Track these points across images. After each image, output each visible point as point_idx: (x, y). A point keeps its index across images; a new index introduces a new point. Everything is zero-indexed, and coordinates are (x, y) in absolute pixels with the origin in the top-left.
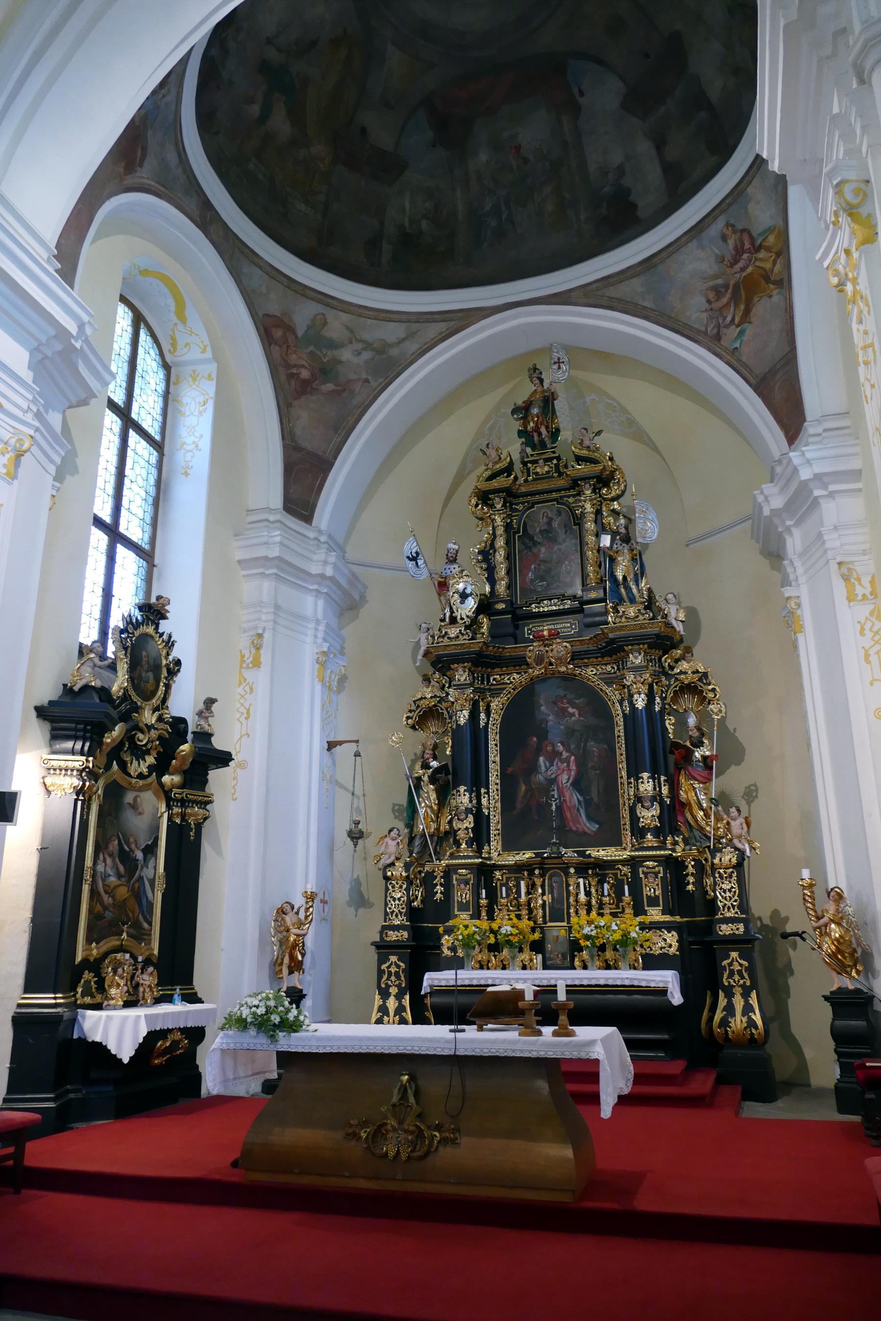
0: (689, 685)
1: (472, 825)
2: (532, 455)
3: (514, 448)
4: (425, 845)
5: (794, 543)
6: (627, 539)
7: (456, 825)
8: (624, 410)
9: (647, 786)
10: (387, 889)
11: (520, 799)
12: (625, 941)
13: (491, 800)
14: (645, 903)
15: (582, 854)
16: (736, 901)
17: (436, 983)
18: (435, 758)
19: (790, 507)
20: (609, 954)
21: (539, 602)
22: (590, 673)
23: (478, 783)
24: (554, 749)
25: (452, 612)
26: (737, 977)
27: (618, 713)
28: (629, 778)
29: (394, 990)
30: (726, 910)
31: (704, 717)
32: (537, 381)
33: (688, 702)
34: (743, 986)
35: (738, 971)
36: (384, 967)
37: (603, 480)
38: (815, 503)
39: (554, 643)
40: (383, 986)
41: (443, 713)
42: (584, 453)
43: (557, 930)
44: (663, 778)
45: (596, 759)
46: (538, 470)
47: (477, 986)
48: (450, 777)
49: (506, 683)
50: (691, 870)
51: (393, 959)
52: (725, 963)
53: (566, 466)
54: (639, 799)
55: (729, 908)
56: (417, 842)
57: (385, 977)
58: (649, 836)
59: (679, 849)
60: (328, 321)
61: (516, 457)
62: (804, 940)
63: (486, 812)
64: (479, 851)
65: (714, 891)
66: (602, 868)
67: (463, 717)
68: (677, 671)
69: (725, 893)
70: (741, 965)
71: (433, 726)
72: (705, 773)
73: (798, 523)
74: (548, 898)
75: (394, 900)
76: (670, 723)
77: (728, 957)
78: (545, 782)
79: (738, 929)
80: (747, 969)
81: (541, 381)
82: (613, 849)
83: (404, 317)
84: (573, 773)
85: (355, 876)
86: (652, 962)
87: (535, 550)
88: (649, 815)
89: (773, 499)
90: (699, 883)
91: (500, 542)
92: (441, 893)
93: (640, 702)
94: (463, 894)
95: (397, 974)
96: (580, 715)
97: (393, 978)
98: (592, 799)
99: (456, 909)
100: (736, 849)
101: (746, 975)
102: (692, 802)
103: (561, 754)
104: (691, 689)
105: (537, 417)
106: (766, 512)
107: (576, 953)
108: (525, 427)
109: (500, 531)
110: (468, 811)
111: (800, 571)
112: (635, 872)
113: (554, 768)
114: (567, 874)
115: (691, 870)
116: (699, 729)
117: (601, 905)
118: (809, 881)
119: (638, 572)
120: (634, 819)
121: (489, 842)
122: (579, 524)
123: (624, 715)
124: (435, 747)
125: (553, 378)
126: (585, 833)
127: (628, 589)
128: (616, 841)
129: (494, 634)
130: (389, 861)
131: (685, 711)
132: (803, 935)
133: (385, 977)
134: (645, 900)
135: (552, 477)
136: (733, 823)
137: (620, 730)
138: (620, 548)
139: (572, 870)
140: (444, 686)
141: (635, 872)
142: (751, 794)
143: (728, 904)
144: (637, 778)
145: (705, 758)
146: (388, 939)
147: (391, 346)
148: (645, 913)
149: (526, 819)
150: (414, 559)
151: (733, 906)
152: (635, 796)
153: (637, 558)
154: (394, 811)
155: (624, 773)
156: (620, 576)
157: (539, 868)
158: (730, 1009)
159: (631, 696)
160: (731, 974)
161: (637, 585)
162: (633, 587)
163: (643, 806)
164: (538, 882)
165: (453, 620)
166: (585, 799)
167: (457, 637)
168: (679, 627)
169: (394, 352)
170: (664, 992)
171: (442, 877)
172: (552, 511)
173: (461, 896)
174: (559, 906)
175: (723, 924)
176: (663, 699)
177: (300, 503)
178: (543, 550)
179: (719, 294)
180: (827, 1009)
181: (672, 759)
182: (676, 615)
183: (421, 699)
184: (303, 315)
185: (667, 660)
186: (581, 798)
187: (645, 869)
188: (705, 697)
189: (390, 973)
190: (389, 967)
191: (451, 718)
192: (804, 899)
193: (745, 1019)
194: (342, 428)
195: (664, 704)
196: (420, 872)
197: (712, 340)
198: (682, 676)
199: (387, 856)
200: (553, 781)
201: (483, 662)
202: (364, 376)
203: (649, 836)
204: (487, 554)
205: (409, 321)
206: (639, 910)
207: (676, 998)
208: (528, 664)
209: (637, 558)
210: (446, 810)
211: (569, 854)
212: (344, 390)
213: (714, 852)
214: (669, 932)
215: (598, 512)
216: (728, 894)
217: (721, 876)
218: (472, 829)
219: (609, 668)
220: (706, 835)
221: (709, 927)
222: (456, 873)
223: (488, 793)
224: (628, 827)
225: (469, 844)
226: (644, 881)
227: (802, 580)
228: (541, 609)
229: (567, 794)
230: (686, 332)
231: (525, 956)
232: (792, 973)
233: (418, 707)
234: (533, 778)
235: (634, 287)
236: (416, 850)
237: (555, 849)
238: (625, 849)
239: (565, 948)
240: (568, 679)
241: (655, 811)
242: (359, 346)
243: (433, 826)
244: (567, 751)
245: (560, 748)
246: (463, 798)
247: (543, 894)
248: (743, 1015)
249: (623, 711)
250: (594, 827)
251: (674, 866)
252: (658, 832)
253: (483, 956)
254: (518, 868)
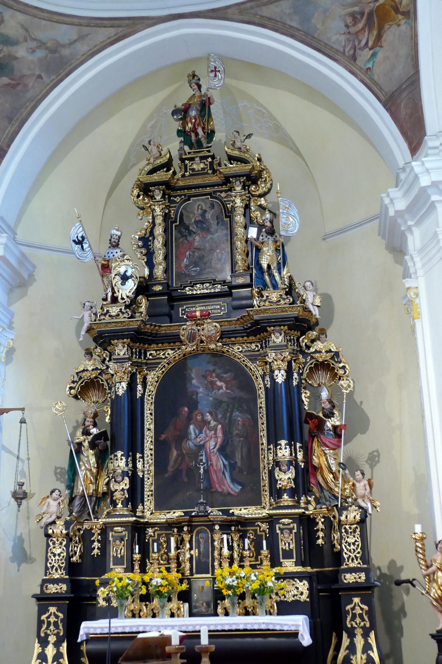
0: (322, 363)
1: (128, 487)
2: (189, 153)
3: (173, 146)
4: (84, 505)
5: (414, 241)
6: (271, 232)
7: (113, 486)
8: (272, 117)
9: (284, 452)
10: (48, 546)
11: (172, 462)
12: (262, 590)
13: (146, 466)
14: (281, 556)
15: (226, 512)
16: (359, 553)
17: (92, 631)
18: (95, 425)
19: (411, 209)
20: (248, 602)
21: (193, 286)
22: (237, 350)
23: (134, 448)
24: (203, 419)
25: (113, 292)
26: (358, 620)
27: (259, 384)
28: (269, 444)
29: (52, 639)
30: (350, 561)
31: (335, 391)
32: (196, 87)
33: (322, 377)
34: (364, 628)
35: (359, 614)
36: (43, 617)
37: (252, 179)
38: (433, 206)
39: (204, 324)
40: (42, 635)
41: (103, 385)
42: (236, 153)
43: (202, 581)
44: (298, 445)
45: (240, 428)
46: (195, 166)
47: (129, 633)
48: (109, 443)
49: (161, 358)
50: (321, 526)
51: (53, 609)
52: (349, 607)
53: (219, 164)
54: (277, 464)
55: (353, 559)
56: (77, 502)
57: (45, 626)
58: (285, 497)
59: (311, 507)
60: (5, 18)
61: (175, 154)
62: (414, 586)
63: (140, 474)
64: (134, 510)
65: (340, 545)
66: (243, 524)
67: (122, 388)
68: (312, 350)
69: (349, 545)
70: (362, 609)
71: (94, 396)
72: (335, 441)
73: (418, 224)
74: (195, 552)
75: (55, 555)
76: (305, 397)
77: (351, 602)
78: (195, 448)
79: (360, 578)
80: (367, 613)
81: (199, 87)
82: (254, 508)
83: (76, 20)
84: (220, 440)
85: (18, 534)
86: (285, 608)
87: (190, 239)
88: (285, 478)
89: (398, 201)
90: (328, 537)
91: (159, 231)
92: (98, 548)
93: (280, 377)
94: (117, 549)
95: (56, 624)
96: (227, 388)
97: (52, 628)
98: (236, 463)
99: (111, 563)
100: (360, 507)
101: (366, 618)
102: (323, 466)
103: (209, 423)
104: (324, 366)
106: (391, 213)
107: (219, 602)
108: (184, 128)
109: (159, 220)
110: (124, 474)
111: (419, 265)
112: (272, 529)
113: (203, 435)
114: (212, 531)
115: (321, 526)
116: (330, 401)
117: (242, 558)
118: (421, 535)
119: (281, 261)
120: (273, 481)
121: (143, 502)
122: (229, 217)
123: (266, 389)
124: (96, 415)
125: (211, 85)
126: (229, 494)
127: (271, 276)
129: (151, 314)
130: (51, 520)
131: (319, 385)
132: (414, 582)
133: (45, 626)
134: (281, 553)
135: (207, 173)
136: (357, 484)
137: (262, 401)
138: (266, 239)
139: (217, 527)
140: (105, 359)
141: (272, 529)
142: (374, 459)
143: (352, 555)
144: (276, 445)
145: (335, 427)
146: (48, 592)
147: (63, 46)
148: (280, 565)
150: (80, 242)
151: (357, 558)
152: (274, 461)
153: (280, 250)
154: (56, 474)
155: (265, 441)
156: (265, 266)
157: (188, 526)
158: (352, 648)
159: (272, 371)
160: (354, 617)
161: (280, 273)
162: (276, 274)
163: (280, 470)
164: (187, 538)
165: (115, 300)
166: (230, 464)
167: (118, 315)
168: (315, 312)
169: (66, 52)
170: (295, 634)
171: (99, 534)
172: (206, 203)
173: (117, 551)
174: (205, 560)
175: (347, 573)
176: (300, 375)
178: (197, 238)
179: (355, 21)
180: (434, 646)
181: (306, 427)
182: (312, 301)
183: (84, 371)
185: (304, 341)
186: (226, 463)
187: (281, 526)
188: (336, 374)
189: (49, 623)
190: (48, 617)
191: (110, 389)
192: (416, 551)
193: (364, 657)
195: (301, 379)
196: (79, 530)
197: (349, 61)
198: (317, 355)
199: (48, 515)
200: (202, 447)
201: (140, 339)
202: (38, 72)
203: (285, 497)
204: (146, 241)
205: (81, 25)
206: (275, 562)
207: (306, 640)
208: (181, 342)
209: (280, 250)
210: (104, 473)
211: (215, 512)
212: (19, 84)
213: (341, 510)
214: (301, 581)
215: (247, 207)
216: (352, 547)
217: (346, 532)
218: (128, 490)
219: (253, 346)
220: (334, 496)
221: (335, 576)
222: (112, 531)
223: (143, 458)
224: (267, 488)
225: (125, 504)
226: (280, 537)
227: (420, 273)
228: (195, 292)
229: (214, 459)
230: (328, 52)
231: (174, 605)
232: (405, 615)
233: (81, 378)
234: (183, 444)
236: (76, 510)
237: (202, 508)
238: (264, 508)
239: (209, 597)
240: (216, 355)
241: (291, 474)
242: (34, 44)
243: (92, 487)
244: (214, 420)
245: (209, 417)
246: (120, 462)
247: (191, 549)
248: (363, 653)
249: (265, 385)
250: (237, 488)
251: (306, 522)
252: (293, 493)
253: (135, 606)
254: (169, 526)
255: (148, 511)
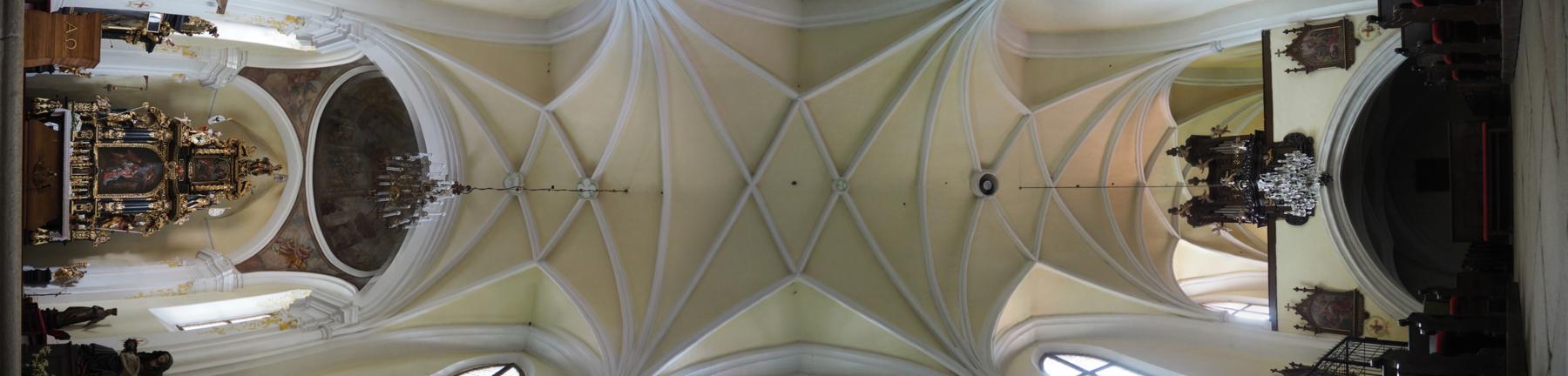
3: (253, 157)
9: (120, 207)
13: (118, 144)
22: (162, 186)
23: (125, 140)
37: (234, 193)
39: (174, 171)
66: (92, 186)
67: (152, 135)
88: (109, 207)
105: (264, 167)
128: (99, 192)
149: (111, 157)
177: (246, 72)
184: (318, 85)
194: (273, 92)
197: (276, 240)
235: (301, 213)
254: (91, 155)
255: (99, 144)
